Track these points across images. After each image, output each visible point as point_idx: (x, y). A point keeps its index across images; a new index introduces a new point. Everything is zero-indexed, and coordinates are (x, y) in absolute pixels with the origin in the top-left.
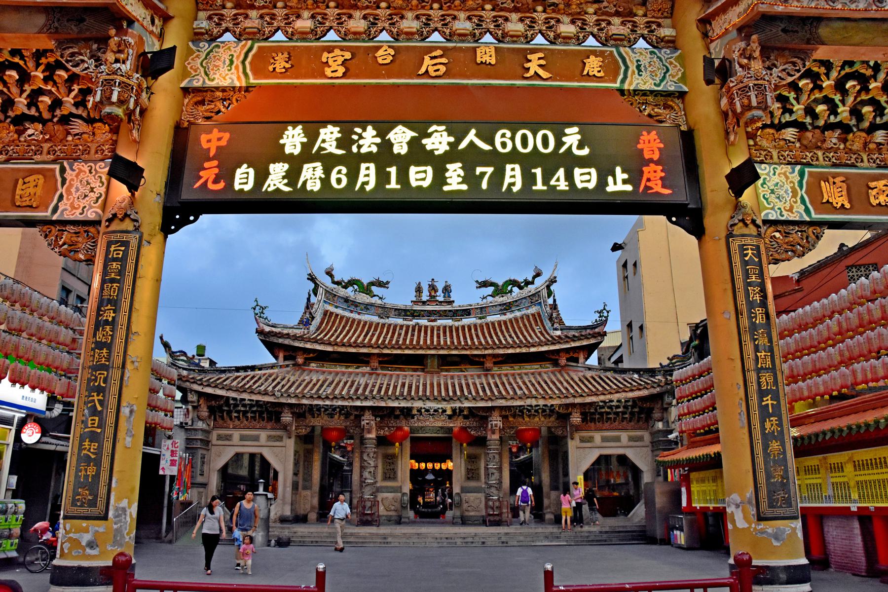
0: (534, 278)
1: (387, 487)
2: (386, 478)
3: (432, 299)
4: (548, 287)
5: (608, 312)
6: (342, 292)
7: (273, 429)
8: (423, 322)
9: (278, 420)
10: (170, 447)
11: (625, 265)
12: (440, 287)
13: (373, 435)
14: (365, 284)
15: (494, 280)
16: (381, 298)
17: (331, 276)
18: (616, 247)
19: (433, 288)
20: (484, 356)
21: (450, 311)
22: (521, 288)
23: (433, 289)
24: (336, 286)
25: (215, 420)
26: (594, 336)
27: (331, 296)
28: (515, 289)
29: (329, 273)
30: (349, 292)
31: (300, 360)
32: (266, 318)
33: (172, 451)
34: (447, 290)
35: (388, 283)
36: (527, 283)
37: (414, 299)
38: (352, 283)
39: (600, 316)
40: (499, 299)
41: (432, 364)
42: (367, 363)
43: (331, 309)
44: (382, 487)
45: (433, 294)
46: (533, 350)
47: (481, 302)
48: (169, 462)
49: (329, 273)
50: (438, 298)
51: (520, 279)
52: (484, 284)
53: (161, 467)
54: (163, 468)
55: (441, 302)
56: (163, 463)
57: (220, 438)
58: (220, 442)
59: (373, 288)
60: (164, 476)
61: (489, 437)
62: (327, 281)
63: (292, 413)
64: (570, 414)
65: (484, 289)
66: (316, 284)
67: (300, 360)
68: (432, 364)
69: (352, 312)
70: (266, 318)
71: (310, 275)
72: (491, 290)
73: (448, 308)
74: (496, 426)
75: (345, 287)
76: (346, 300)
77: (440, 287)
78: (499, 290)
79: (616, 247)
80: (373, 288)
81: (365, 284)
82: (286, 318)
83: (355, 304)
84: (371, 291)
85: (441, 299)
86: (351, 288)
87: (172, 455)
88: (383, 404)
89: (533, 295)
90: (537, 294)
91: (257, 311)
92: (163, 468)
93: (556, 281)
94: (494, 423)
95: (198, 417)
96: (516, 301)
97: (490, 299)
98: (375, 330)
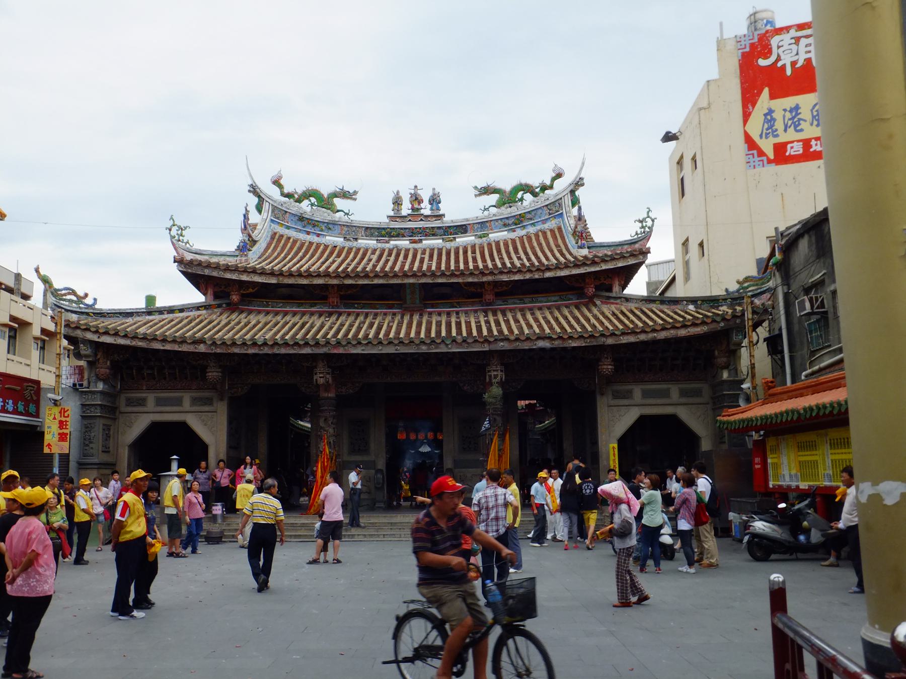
0: (554, 179)
2: (353, 451)
3: (416, 213)
4: (572, 192)
5: (653, 221)
7: (199, 389)
8: (404, 243)
9: (204, 378)
10: (58, 416)
11: (680, 163)
12: (426, 196)
14: (326, 196)
15: (499, 185)
16: (347, 214)
17: (280, 186)
18: (669, 137)
19: (416, 199)
20: (482, 284)
21: (439, 228)
22: (535, 195)
23: (416, 199)
25: (122, 379)
26: (633, 255)
27: (279, 214)
28: (528, 197)
29: (277, 183)
30: (305, 206)
31: (235, 298)
32: (188, 242)
33: (61, 422)
34: (435, 200)
35: (355, 193)
36: (544, 188)
37: (392, 214)
39: (643, 227)
40: (506, 212)
42: (324, 298)
43: (281, 230)
45: (416, 206)
46: (548, 275)
47: (479, 214)
48: (57, 437)
49: (277, 183)
50: (422, 211)
51: (535, 182)
52: (486, 191)
53: (46, 443)
54: (49, 445)
55: (427, 216)
56: (48, 438)
57: (130, 402)
58: (129, 409)
59: (336, 201)
60: (51, 456)
62: (273, 192)
63: (220, 367)
64: (599, 360)
65: (485, 197)
66: (259, 197)
67: (235, 298)
69: (308, 233)
70: (188, 242)
71: (251, 186)
72: (494, 198)
73: (437, 224)
74: (496, 376)
75: (299, 201)
76: (301, 218)
77: (426, 196)
79: (669, 137)
80: (336, 201)
81: (326, 196)
82: (219, 241)
83: (314, 223)
84: (333, 204)
86: (306, 203)
87: (61, 427)
89: (553, 203)
90: (558, 203)
91: (174, 232)
92: (49, 445)
93: (583, 185)
95: (97, 376)
97: (494, 210)
98: (339, 256)
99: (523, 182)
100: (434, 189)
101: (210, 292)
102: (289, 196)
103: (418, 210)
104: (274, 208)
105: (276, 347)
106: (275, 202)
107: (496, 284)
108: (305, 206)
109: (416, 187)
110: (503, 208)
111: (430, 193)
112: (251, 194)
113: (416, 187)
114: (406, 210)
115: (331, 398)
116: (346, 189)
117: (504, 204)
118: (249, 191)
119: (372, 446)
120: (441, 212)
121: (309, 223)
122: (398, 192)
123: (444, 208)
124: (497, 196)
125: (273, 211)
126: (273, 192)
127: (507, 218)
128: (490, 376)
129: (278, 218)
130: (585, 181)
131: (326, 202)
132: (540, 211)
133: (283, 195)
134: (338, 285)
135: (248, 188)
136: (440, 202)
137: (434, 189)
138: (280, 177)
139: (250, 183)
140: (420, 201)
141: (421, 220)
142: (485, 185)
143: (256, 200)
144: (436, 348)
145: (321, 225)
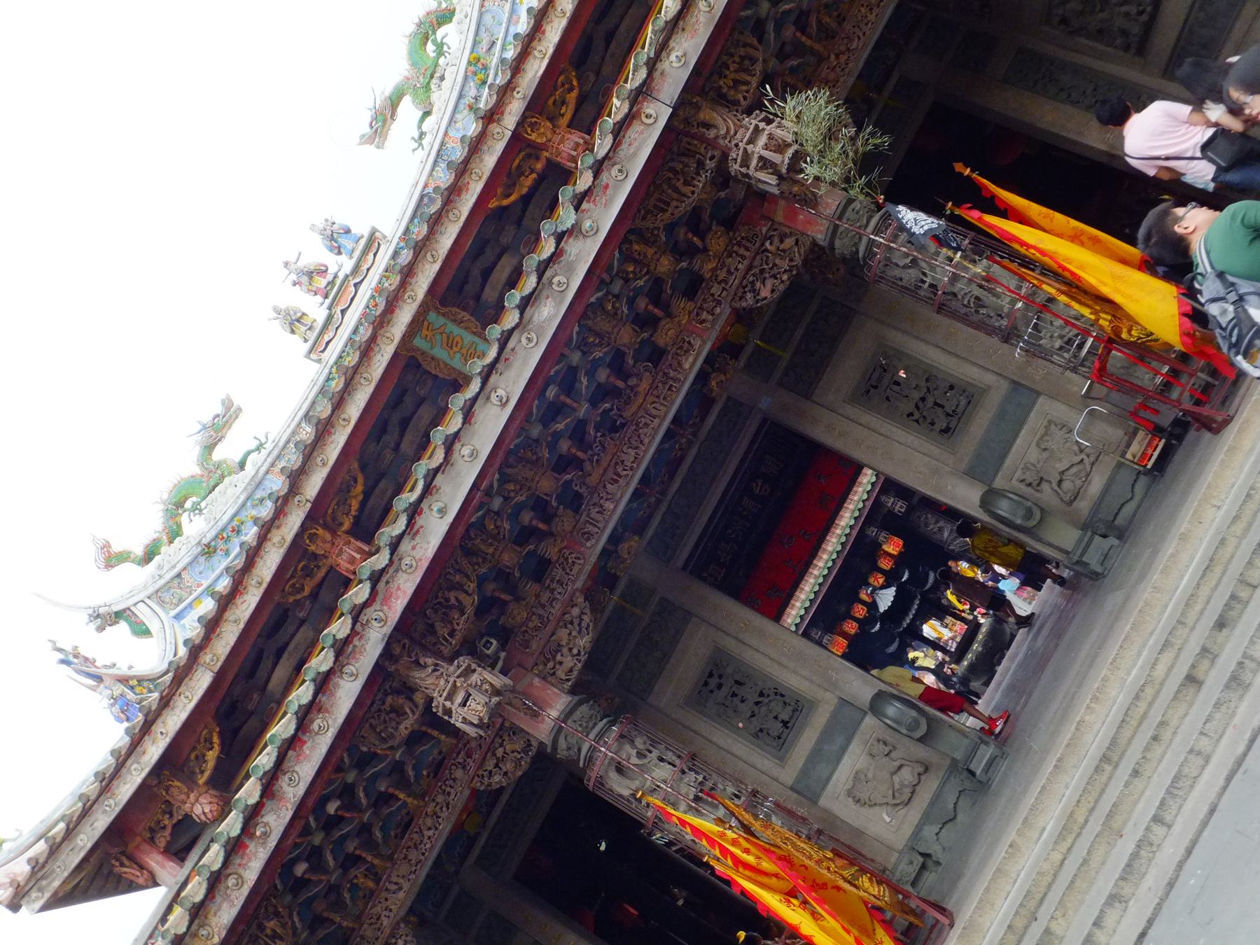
1: (816, 755)
3: (335, 293)
6: (176, 555)
12: (317, 253)
13: (557, 704)
15: (387, 87)
16: (259, 448)
17: (123, 557)
23: (310, 274)
24: (157, 558)
29: (112, 559)
30: (195, 528)
34: (335, 238)
35: (228, 404)
38: (176, 506)
44: (805, 772)
45: (321, 282)
47: (421, 154)
49: (112, 559)
59: (218, 454)
61: (819, 233)
66: (118, 616)
72: (408, 110)
75: (174, 533)
77: (317, 253)
78: (424, 79)
84: (218, 466)
85: (348, 264)
88: (405, 586)
96: (475, 43)
97: (430, 122)
99: (411, 28)
100: (313, 227)
101: (155, 861)
103: (332, 283)
104: (157, 595)
105: (283, 783)
106: (145, 587)
107: (538, 106)
110: (435, 97)
112: (108, 628)
113: (286, 264)
114: (316, 310)
115: (567, 715)
116: (207, 419)
117: (427, 87)
118: (101, 629)
119: (794, 680)
120: (366, 234)
121: (227, 540)
122: (277, 311)
124: (407, 102)
125: (161, 602)
127: (460, 96)
128: (765, 164)
129: (181, 601)
131: (213, 476)
132: (488, 19)
134: (310, 518)
135: (93, 626)
136: (348, 231)
137: (313, 227)
138: (107, 545)
139: (86, 618)
140: (323, 271)
141: (357, 285)
142: (367, 116)
143: (123, 626)
144: (570, 270)
145: (242, 517)
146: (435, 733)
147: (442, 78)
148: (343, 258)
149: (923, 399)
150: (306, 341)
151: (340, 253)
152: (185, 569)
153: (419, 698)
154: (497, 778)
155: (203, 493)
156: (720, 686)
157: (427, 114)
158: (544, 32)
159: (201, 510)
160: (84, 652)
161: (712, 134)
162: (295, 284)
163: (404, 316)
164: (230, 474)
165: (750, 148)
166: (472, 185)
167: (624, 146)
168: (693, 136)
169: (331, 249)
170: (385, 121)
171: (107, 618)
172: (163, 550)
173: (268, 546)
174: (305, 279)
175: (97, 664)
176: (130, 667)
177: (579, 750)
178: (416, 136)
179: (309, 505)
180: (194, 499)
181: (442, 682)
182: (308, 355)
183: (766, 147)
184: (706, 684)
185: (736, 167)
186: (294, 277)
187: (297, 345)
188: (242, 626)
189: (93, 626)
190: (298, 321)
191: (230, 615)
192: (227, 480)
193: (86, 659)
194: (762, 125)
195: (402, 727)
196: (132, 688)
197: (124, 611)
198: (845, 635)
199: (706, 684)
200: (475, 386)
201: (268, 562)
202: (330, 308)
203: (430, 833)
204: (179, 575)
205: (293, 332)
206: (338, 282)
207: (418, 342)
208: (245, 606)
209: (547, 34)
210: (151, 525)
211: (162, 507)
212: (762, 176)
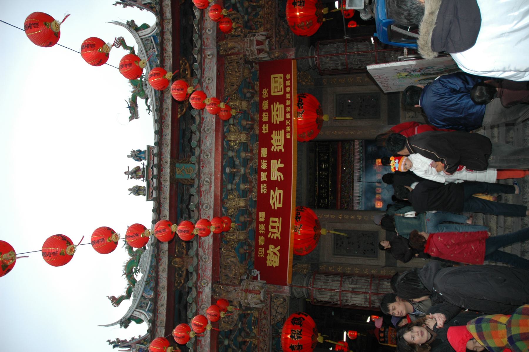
6: (139, 289)
12: (134, 164)
14: (131, 257)
17: (122, 298)
19: (135, 173)
24: (132, 293)
30: (139, 277)
34: (137, 155)
38: (129, 274)
41: (185, 172)
45: (140, 173)
47: (151, 113)
52: (133, 107)
62: (127, 305)
68: (185, 172)
72: (140, 102)
77: (134, 164)
93: (133, 21)
94: (255, 47)
100: (128, 156)
102: (129, 293)
103: (143, 172)
108: (139, 277)
109: (126, 173)
111: (131, 159)
113: (126, 173)
114: (142, 183)
118: (126, 327)
120: (146, 148)
122: (130, 190)
123: (144, 148)
124: (138, 99)
126: (127, 305)
130: (130, 20)
133: (128, 296)
137: (128, 156)
139: (119, 325)
140: (138, 169)
143: (133, 323)
146: (249, 312)
147: (146, 85)
148: (143, 161)
149: (361, 106)
150: (145, 195)
151: (141, 160)
152: (143, 293)
153: (235, 303)
154: (279, 317)
155: (136, 264)
156: (343, 243)
157: (147, 99)
158: (166, 50)
159: (139, 270)
160: (122, 339)
161: (236, 50)
162: (131, 178)
163: (167, 170)
164: (142, 253)
165: (252, 48)
166: (167, 113)
167: (206, 70)
168: (231, 55)
169: (138, 160)
170: (134, 109)
171: (125, 323)
172: (133, 290)
173: (160, 273)
174: (134, 174)
175: (128, 341)
176: (140, 336)
177: (303, 292)
178: (147, 108)
179: (167, 252)
180: (135, 268)
181: (240, 294)
182: (147, 200)
183: (257, 45)
184: (337, 244)
185: (251, 57)
186: (130, 176)
187: (142, 198)
188: (165, 306)
189: (123, 328)
190: (139, 190)
191: (159, 303)
192: (142, 256)
193: (123, 341)
194: (252, 38)
195: (234, 317)
196: (142, 344)
197: (130, 317)
198: (343, 217)
199: (337, 244)
200: (196, 182)
201: (164, 279)
202: (147, 180)
203: (265, 348)
204: (142, 296)
205: (139, 195)
206: (145, 170)
207: (177, 176)
208: (163, 298)
209: (167, 49)
210: (124, 283)
211: (125, 276)
212: (261, 55)
